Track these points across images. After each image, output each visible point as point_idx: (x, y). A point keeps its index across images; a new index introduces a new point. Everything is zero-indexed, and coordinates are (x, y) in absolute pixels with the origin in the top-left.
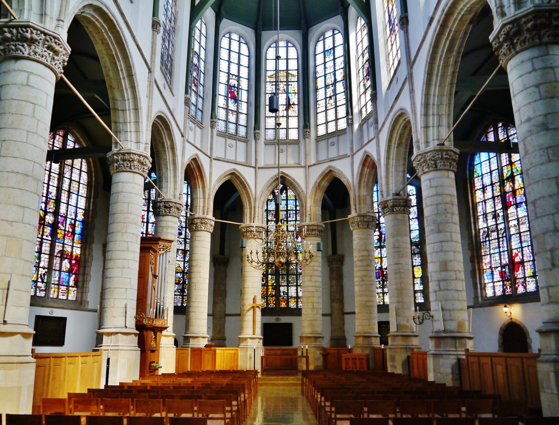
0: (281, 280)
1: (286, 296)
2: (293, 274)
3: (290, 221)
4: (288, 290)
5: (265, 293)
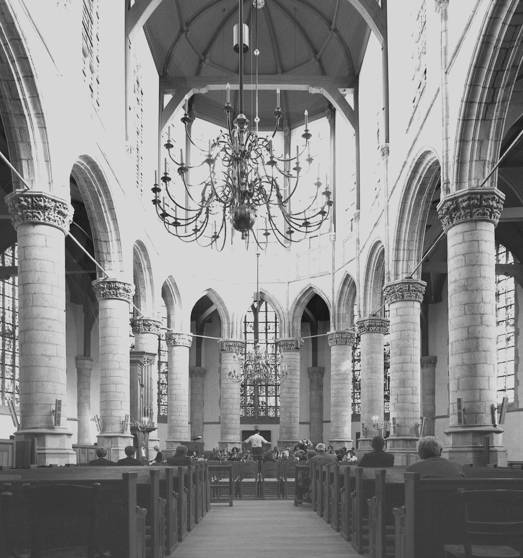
0: (259, 390)
1: (265, 405)
2: (272, 385)
4: (267, 400)
5: (243, 402)
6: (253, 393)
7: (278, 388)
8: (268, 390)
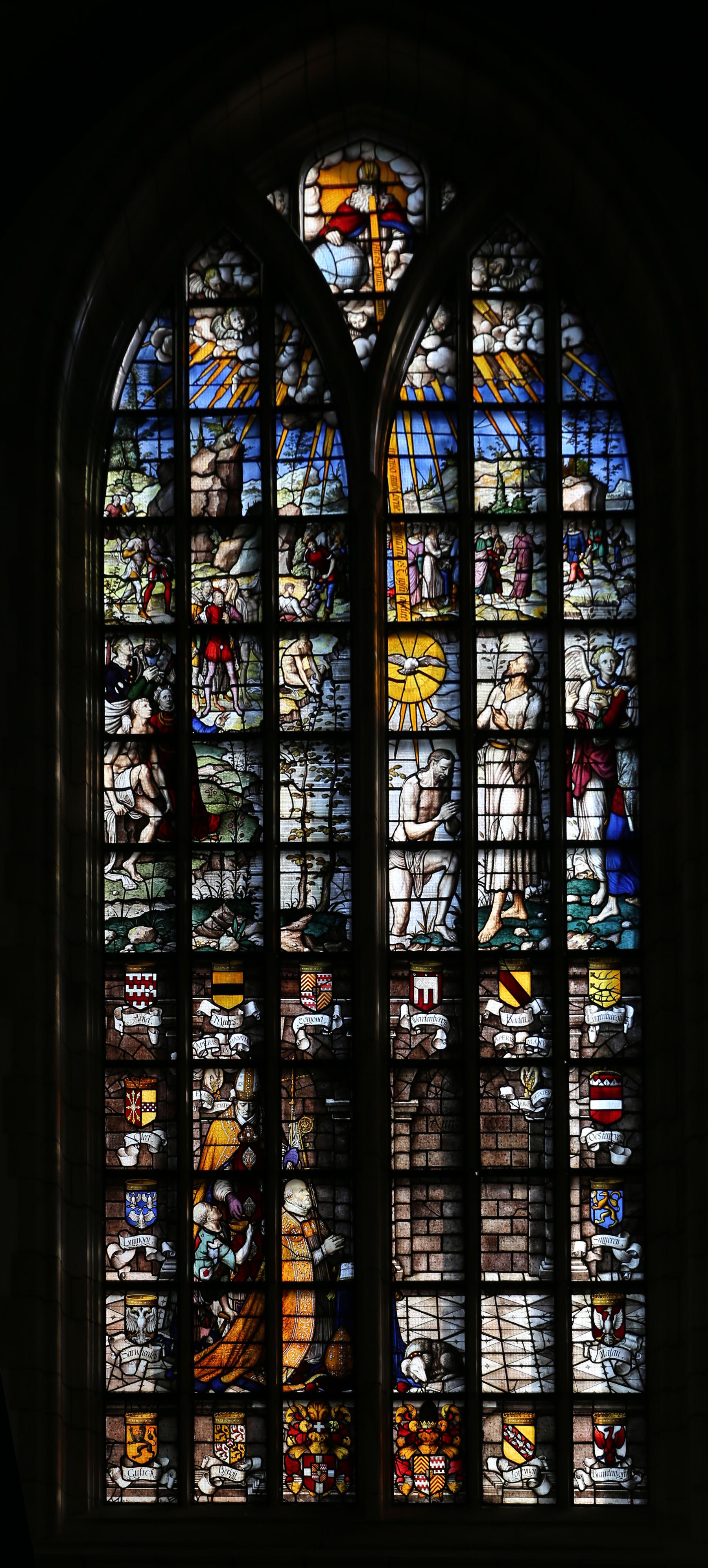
0: (404, 1229)
1: (453, 1387)
3: (499, 629)
6: (332, 1261)
7: (585, 1200)
8: (489, 1226)
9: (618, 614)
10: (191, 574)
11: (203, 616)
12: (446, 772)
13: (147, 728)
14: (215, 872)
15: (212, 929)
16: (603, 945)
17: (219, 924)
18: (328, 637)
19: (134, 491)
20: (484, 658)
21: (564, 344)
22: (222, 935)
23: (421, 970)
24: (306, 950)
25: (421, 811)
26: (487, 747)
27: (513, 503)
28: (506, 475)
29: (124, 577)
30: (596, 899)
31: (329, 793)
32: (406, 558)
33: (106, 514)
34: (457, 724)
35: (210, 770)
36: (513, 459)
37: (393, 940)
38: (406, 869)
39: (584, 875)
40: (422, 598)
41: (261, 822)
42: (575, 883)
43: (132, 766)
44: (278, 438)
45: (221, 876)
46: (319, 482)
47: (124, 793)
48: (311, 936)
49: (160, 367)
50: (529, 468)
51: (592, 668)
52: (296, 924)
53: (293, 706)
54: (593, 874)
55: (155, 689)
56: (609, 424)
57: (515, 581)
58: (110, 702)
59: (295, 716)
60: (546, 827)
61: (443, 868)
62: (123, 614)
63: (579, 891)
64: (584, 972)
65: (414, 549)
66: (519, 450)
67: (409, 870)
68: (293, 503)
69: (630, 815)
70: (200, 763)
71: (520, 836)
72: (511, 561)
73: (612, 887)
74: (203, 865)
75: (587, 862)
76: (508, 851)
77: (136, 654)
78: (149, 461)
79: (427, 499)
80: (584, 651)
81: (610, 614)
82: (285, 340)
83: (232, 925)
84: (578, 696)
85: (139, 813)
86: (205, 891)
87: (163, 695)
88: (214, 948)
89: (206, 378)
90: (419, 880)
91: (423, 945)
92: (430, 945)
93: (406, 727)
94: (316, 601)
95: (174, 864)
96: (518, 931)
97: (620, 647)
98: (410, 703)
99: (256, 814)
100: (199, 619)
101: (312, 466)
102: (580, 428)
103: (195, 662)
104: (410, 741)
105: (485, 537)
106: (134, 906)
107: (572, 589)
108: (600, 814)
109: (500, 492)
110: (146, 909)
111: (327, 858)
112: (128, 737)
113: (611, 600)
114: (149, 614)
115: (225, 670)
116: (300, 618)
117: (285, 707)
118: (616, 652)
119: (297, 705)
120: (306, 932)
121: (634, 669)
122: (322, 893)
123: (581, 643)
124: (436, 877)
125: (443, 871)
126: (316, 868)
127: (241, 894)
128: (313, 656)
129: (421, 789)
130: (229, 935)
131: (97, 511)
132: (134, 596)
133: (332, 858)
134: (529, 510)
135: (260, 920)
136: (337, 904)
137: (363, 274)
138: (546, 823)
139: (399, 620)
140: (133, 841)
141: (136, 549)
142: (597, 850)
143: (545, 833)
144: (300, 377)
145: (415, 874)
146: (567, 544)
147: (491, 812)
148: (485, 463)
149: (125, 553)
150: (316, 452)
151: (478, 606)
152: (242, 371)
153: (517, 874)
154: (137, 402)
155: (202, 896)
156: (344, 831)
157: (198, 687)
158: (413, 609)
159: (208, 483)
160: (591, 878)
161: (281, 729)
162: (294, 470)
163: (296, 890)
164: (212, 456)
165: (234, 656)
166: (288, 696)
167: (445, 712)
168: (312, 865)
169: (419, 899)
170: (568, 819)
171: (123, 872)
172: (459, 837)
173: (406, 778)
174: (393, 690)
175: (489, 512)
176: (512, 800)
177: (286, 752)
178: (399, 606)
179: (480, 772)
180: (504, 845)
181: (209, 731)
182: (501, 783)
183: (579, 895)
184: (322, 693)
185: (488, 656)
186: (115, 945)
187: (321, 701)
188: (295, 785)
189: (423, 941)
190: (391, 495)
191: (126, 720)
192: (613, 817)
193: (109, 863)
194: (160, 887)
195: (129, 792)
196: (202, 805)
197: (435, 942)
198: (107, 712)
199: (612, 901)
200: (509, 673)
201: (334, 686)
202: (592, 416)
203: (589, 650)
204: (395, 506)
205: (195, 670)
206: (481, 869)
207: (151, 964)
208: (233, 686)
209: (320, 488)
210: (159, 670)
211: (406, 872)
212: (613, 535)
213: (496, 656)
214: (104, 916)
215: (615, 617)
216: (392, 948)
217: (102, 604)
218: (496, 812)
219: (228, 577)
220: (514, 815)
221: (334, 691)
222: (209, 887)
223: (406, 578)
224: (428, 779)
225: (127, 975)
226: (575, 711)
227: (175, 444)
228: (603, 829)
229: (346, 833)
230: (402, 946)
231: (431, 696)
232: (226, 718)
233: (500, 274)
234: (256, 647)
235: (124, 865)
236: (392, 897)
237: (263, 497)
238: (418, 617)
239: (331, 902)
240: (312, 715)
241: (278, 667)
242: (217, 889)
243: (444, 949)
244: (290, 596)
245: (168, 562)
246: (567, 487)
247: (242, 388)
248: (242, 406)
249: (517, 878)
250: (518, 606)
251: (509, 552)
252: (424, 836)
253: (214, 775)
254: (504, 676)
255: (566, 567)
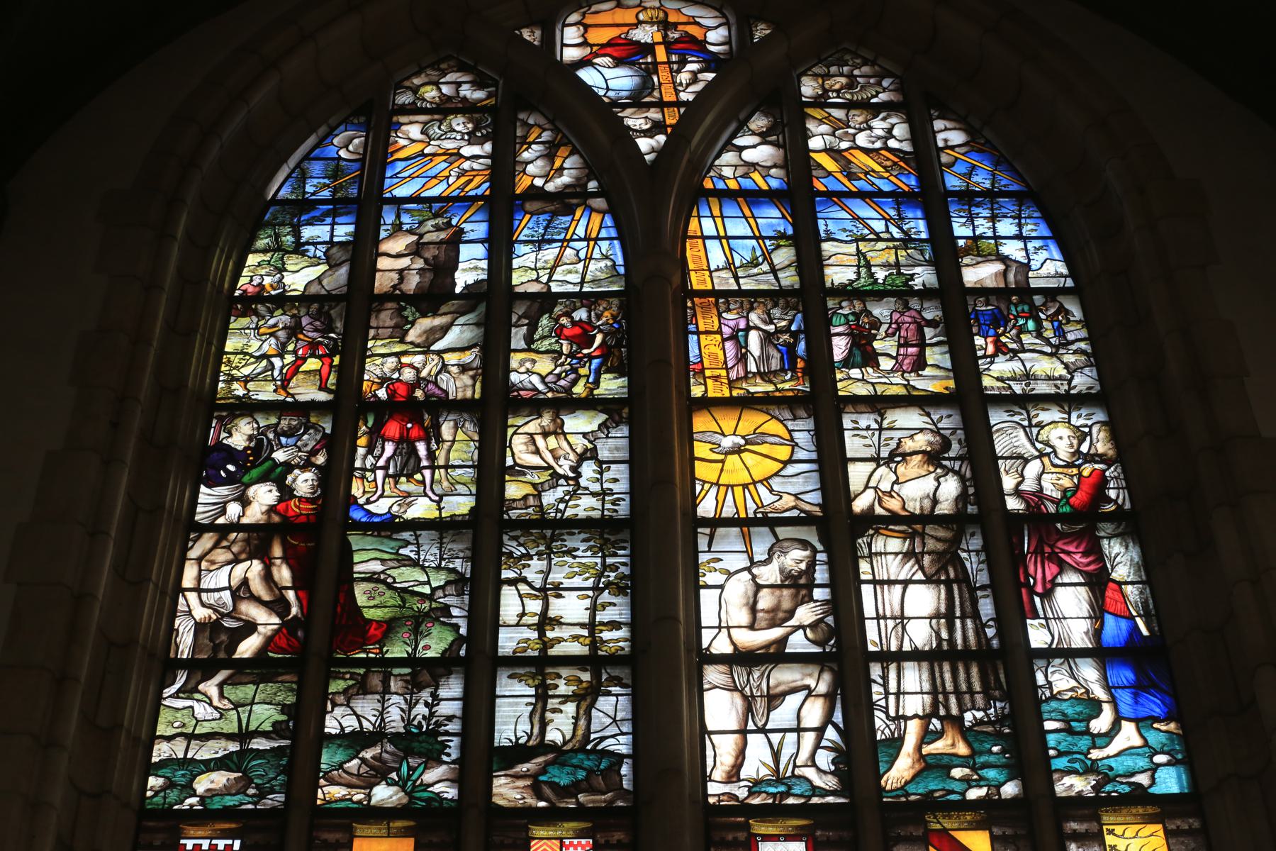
3: (878, 404)
9: (1070, 388)
10: (367, 349)
11: (382, 394)
12: (803, 566)
13: (269, 517)
14: (369, 697)
15: (359, 775)
16: (1127, 789)
17: (372, 767)
18: (592, 413)
19: (286, 271)
20: (854, 435)
21: (941, 144)
22: (378, 784)
23: (771, 830)
24: (542, 804)
25: (760, 615)
26: (872, 536)
27: (884, 280)
28: (869, 255)
29: (257, 354)
30: (1101, 724)
31: (590, 593)
32: (720, 332)
33: (237, 293)
34: (817, 509)
35: (376, 567)
36: (879, 239)
37: (713, 788)
38: (735, 689)
39: (1070, 694)
40: (747, 373)
41: (463, 631)
42: (1054, 704)
43: (236, 561)
44: (517, 223)
45: (383, 701)
46: (580, 260)
47: (217, 595)
48: (553, 785)
49: (343, 163)
50: (906, 248)
51: (1039, 446)
52: (524, 768)
53: (529, 490)
54: (1087, 692)
55: (290, 472)
56: (1020, 210)
57: (898, 354)
58: (209, 486)
59: (531, 501)
60: (990, 632)
61: (807, 687)
62: (249, 391)
63: (1064, 714)
64: (1093, 826)
65: (732, 324)
66: (887, 231)
67: (742, 692)
68: (537, 280)
69: (1139, 615)
70: (356, 558)
71: (945, 644)
72: (887, 335)
73: (1125, 709)
74: (349, 687)
75: (1073, 676)
76: (925, 665)
77: (264, 434)
78: (315, 244)
79: (749, 276)
80: (1024, 427)
81: (1056, 386)
82: (531, 139)
83: (398, 770)
84: (1022, 475)
85: (239, 619)
86: (350, 723)
87: (303, 482)
88: (359, 802)
89: (411, 171)
90: (760, 705)
91: (774, 795)
92: (788, 794)
93: (728, 512)
94: (573, 376)
95: (294, 686)
96: (957, 773)
97: (1081, 422)
98: (732, 486)
99: (454, 621)
100: (375, 396)
101: (568, 246)
102: (978, 214)
103: (362, 441)
104: (735, 531)
105: (846, 312)
106: (211, 743)
107: (992, 363)
108: (1086, 615)
109: (863, 271)
110: (234, 747)
111: (586, 677)
112: (236, 527)
113: (1056, 374)
114: (291, 391)
115: (414, 451)
116: (545, 394)
117: (514, 490)
118: (1078, 427)
119: (535, 489)
120: (542, 778)
121: (1109, 445)
122: (575, 725)
123: (1017, 418)
124: (793, 701)
125: (805, 693)
126: (563, 689)
127: (420, 726)
128: (565, 434)
129: (759, 587)
130: (394, 783)
131: (226, 285)
132: (270, 373)
133: (596, 675)
134: (911, 287)
135: (453, 762)
136: (603, 739)
137: (646, 85)
138: (990, 627)
139: (711, 394)
140: (222, 655)
141: (281, 326)
142: (1089, 660)
143: (988, 640)
144: (552, 169)
145: (752, 696)
146: (977, 320)
147: (888, 614)
148: (836, 243)
149: (262, 331)
150: (574, 233)
151: (841, 380)
152: (466, 165)
153: (946, 694)
154: (305, 193)
155: (342, 729)
156: (618, 641)
157: (364, 469)
158: (731, 384)
159: (405, 262)
160: (1085, 697)
161: (506, 517)
162: (540, 250)
163: (525, 720)
164: (415, 238)
165: (432, 434)
166: (520, 478)
167: (795, 495)
168: (556, 686)
169: (762, 730)
170: (1029, 621)
171: (197, 696)
172: (833, 646)
173: (730, 574)
174: (701, 470)
175: (849, 288)
176: (923, 600)
177: (515, 544)
178: (709, 382)
179: (864, 566)
180: (916, 655)
181: (377, 520)
182: (901, 577)
183: (1066, 719)
184: (579, 475)
185: (864, 433)
186: (165, 798)
187: (578, 484)
188: (530, 584)
189: (772, 790)
190: (692, 274)
191: (234, 510)
192: (1109, 619)
193: (173, 683)
194: (264, 717)
195: (227, 595)
196: (358, 610)
197: (797, 790)
198: (202, 499)
199: (1128, 728)
200: (900, 450)
201: (601, 468)
202: (992, 203)
203: (1030, 426)
204: (697, 281)
205: (361, 451)
206: (876, 689)
207: (233, 826)
208: (425, 468)
209: (580, 266)
210: (300, 451)
211: (737, 696)
212: (1047, 310)
213: (877, 433)
214: (151, 756)
215: (1067, 392)
216: (712, 800)
217: (216, 381)
218: (897, 612)
219: (426, 352)
220: (931, 618)
221: (601, 473)
222: (358, 717)
223: (721, 353)
224: (770, 574)
225: (182, 842)
226: (1017, 493)
227: (356, 229)
228: (1097, 634)
229: (621, 644)
230: (733, 796)
231: (770, 477)
232: (410, 505)
233: (842, 88)
234: (469, 426)
235: (201, 687)
236: (710, 727)
237: (489, 275)
238: (742, 392)
239: (593, 736)
240: (561, 500)
241: (504, 445)
242: (373, 719)
243: (815, 800)
244: (528, 371)
245: (330, 338)
246: (968, 265)
247: (463, 180)
248: (462, 194)
249: (947, 699)
250: (908, 381)
251: (884, 327)
252: (768, 646)
253: (383, 572)
254: (893, 455)
255: (979, 341)
